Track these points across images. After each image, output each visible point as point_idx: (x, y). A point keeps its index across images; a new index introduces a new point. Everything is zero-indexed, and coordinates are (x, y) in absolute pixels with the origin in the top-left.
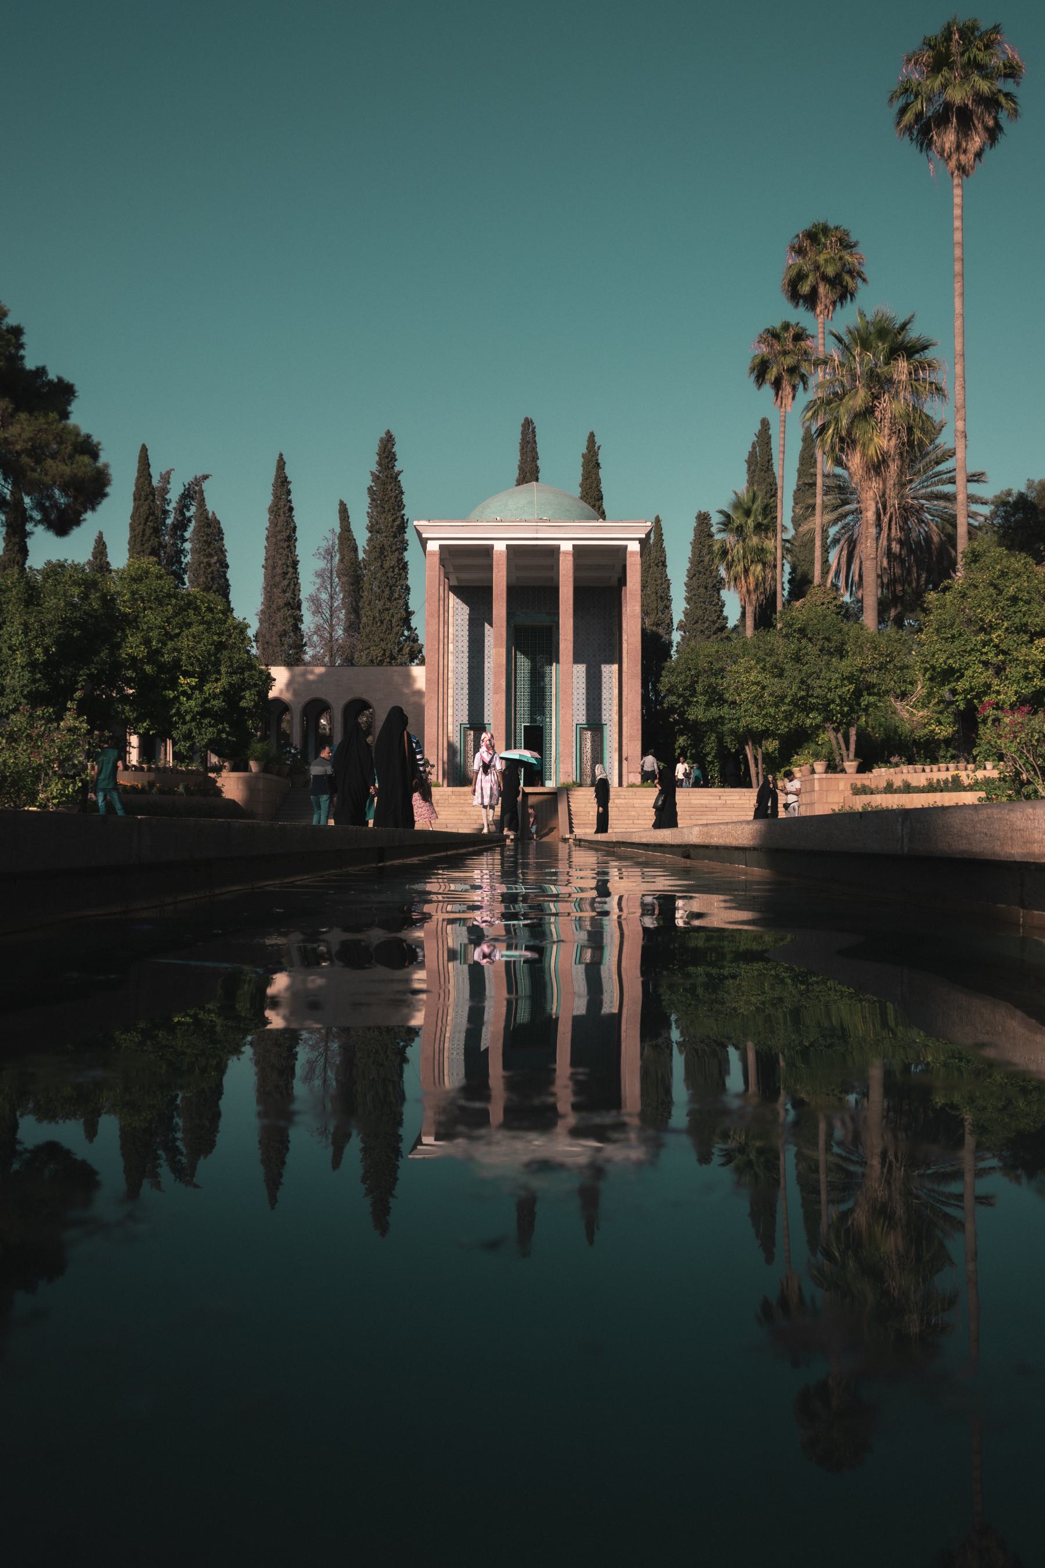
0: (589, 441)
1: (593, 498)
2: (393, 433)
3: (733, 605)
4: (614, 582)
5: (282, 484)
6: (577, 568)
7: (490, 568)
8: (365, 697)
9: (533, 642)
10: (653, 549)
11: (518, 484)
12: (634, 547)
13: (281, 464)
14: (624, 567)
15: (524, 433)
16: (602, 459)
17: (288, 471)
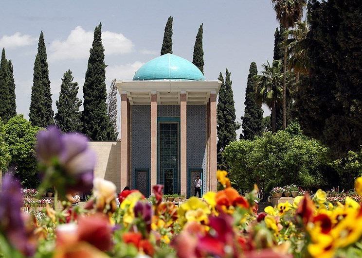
4: (206, 103)
11: (162, 54)
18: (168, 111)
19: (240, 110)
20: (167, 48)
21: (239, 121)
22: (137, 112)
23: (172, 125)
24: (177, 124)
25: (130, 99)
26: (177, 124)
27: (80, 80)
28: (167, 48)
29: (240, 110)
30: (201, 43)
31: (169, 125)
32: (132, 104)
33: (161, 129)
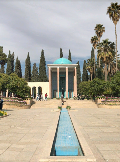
0: (69, 54)
1: (70, 58)
2: (44, 50)
3: (89, 74)
4: (73, 71)
5: (28, 56)
6: (68, 70)
7: (57, 70)
8: (41, 86)
9: (63, 79)
10: (78, 67)
12: (76, 68)
13: (28, 54)
14: (74, 70)
15: (61, 50)
16: (71, 53)
17: (29, 54)
18: (63, 72)
19: (82, 73)
20: (61, 56)
21: (82, 76)
22: (54, 73)
23: (64, 77)
24: (65, 77)
25: (51, 70)
26: (65, 77)
27: (38, 66)
28: (61, 56)
29: (82, 73)
30: (70, 55)
31: (63, 77)
32: (52, 71)
33: (61, 79)
